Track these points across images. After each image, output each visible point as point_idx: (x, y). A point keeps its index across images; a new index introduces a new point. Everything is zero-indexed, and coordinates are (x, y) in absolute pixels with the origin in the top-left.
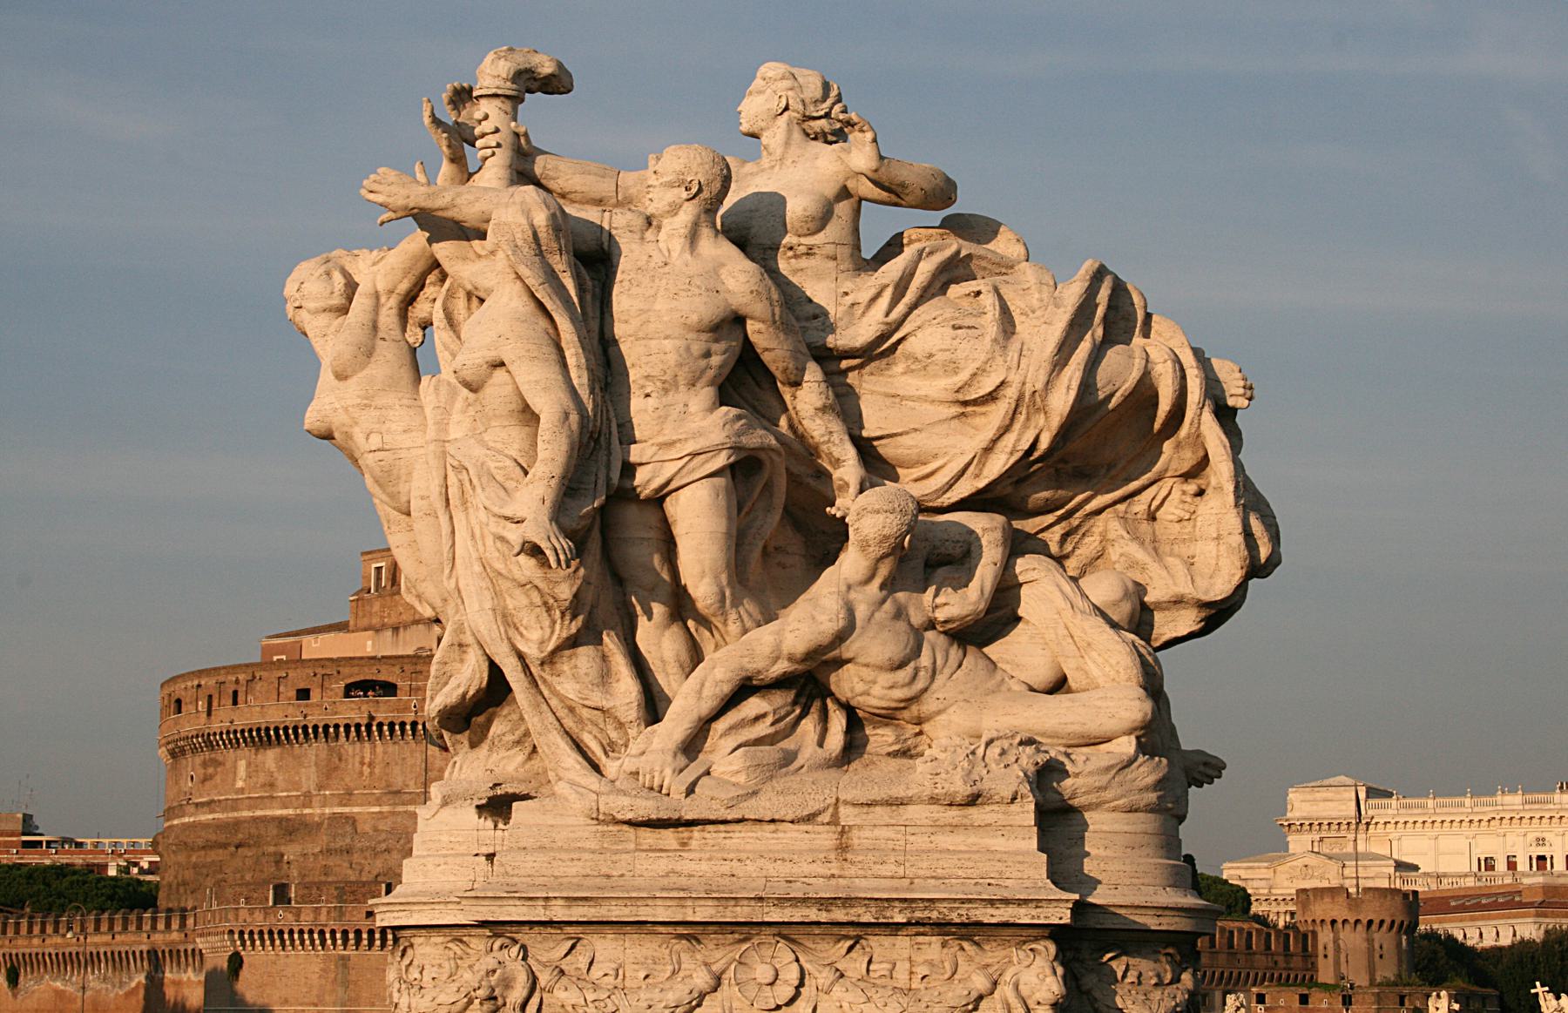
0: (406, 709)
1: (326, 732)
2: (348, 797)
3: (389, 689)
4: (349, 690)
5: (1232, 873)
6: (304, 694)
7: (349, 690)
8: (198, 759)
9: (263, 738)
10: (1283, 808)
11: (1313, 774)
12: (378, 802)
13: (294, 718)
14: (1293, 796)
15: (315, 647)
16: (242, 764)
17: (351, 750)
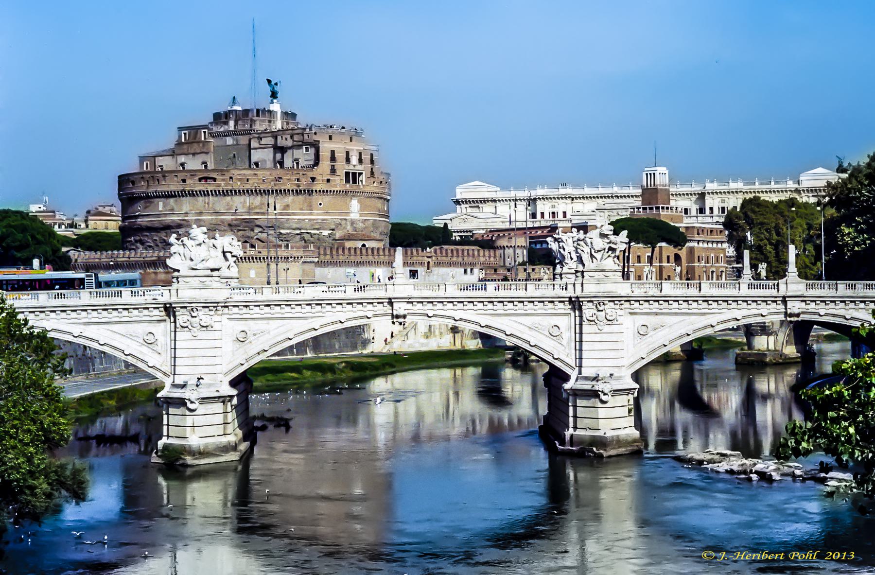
0: (220, 186)
2: (201, 214)
3: (215, 179)
4: (200, 180)
6: (184, 181)
7: (200, 180)
12: (211, 214)
13: (180, 188)
14: (458, 191)
16: (161, 204)
17: (200, 199)
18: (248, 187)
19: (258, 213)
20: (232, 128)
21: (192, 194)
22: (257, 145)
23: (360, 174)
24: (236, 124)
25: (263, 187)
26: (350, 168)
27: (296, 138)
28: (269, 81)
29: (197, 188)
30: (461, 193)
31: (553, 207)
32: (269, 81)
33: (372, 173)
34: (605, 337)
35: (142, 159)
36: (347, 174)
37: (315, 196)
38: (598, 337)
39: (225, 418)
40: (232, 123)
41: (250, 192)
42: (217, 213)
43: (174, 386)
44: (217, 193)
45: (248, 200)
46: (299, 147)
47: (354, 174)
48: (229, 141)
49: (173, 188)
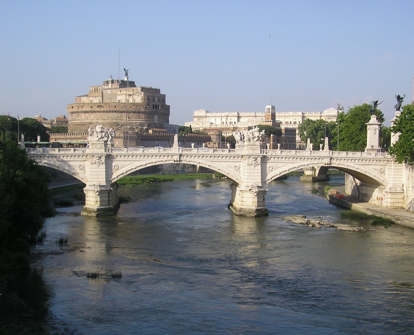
1: (95, 112)
2: (98, 119)
5: (187, 125)
6: (92, 107)
8: (76, 114)
9: (86, 112)
10: (193, 114)
11: (198, 109)
15: (85, 100)
16: (83, 115)
17: (98, 114)
18: (116, 109)
19: (119, 120)
20: (110, 87)
21: (95, 112)
22: (119, 94)
23: (158, 105)
24: (112, 85)
25: (122, 110)
26: (155, 104)
27: (135, 91)
28: (125, 69)
29: (97, 110)
30: (196, 113)
31: (231, 119)
32: (125, 69)
33: (163, 105)
34: (255, 171)
35: (76, 99)
36: (153, 105)
37: (141, 114)
38: (252, 171)
39: (109, 199)
40: (110, 85)
41: (116, 112)
42: (104, 119)
43: (90, 185)
44: (104, 112)
45: (116, 114)
46: (136, 95)
47: (156, 105)
48: (109, 92)
49: (88, 110)
